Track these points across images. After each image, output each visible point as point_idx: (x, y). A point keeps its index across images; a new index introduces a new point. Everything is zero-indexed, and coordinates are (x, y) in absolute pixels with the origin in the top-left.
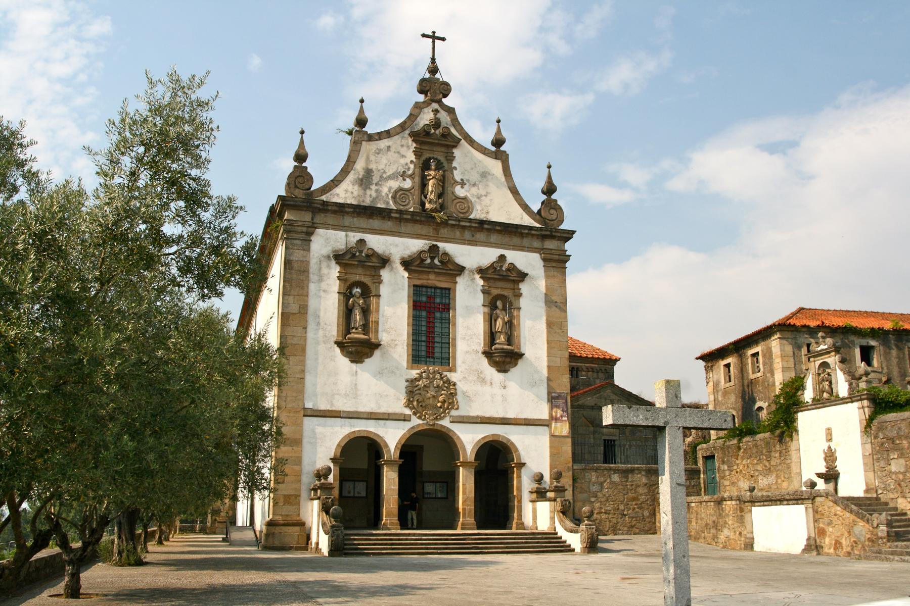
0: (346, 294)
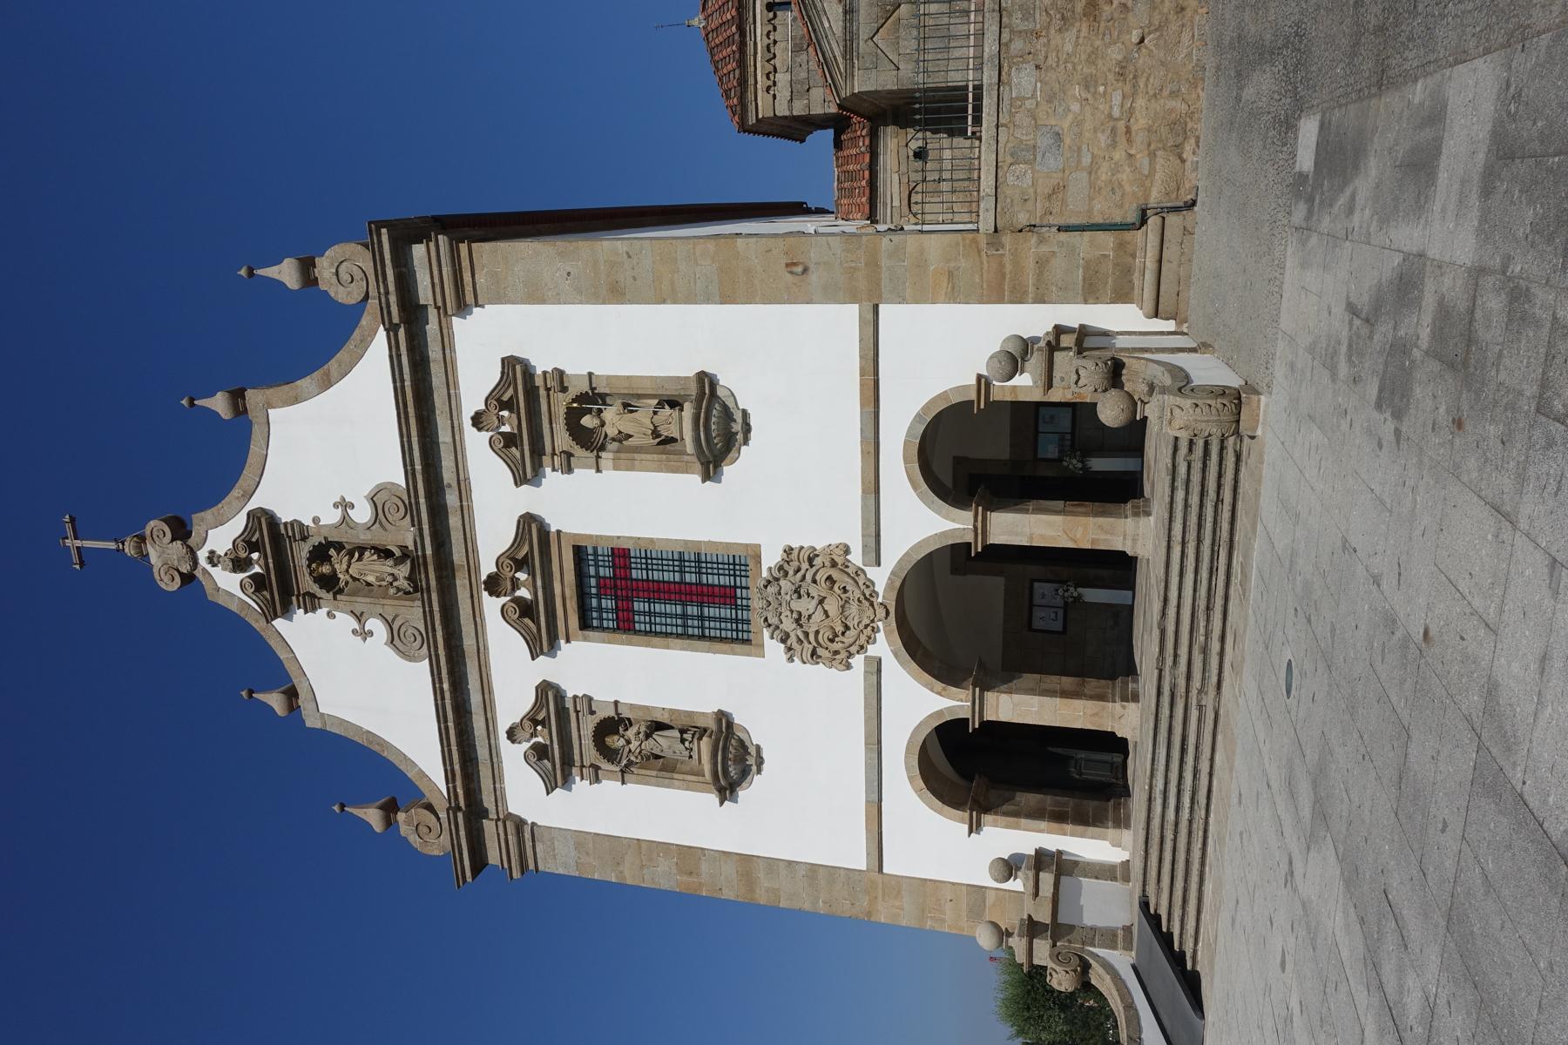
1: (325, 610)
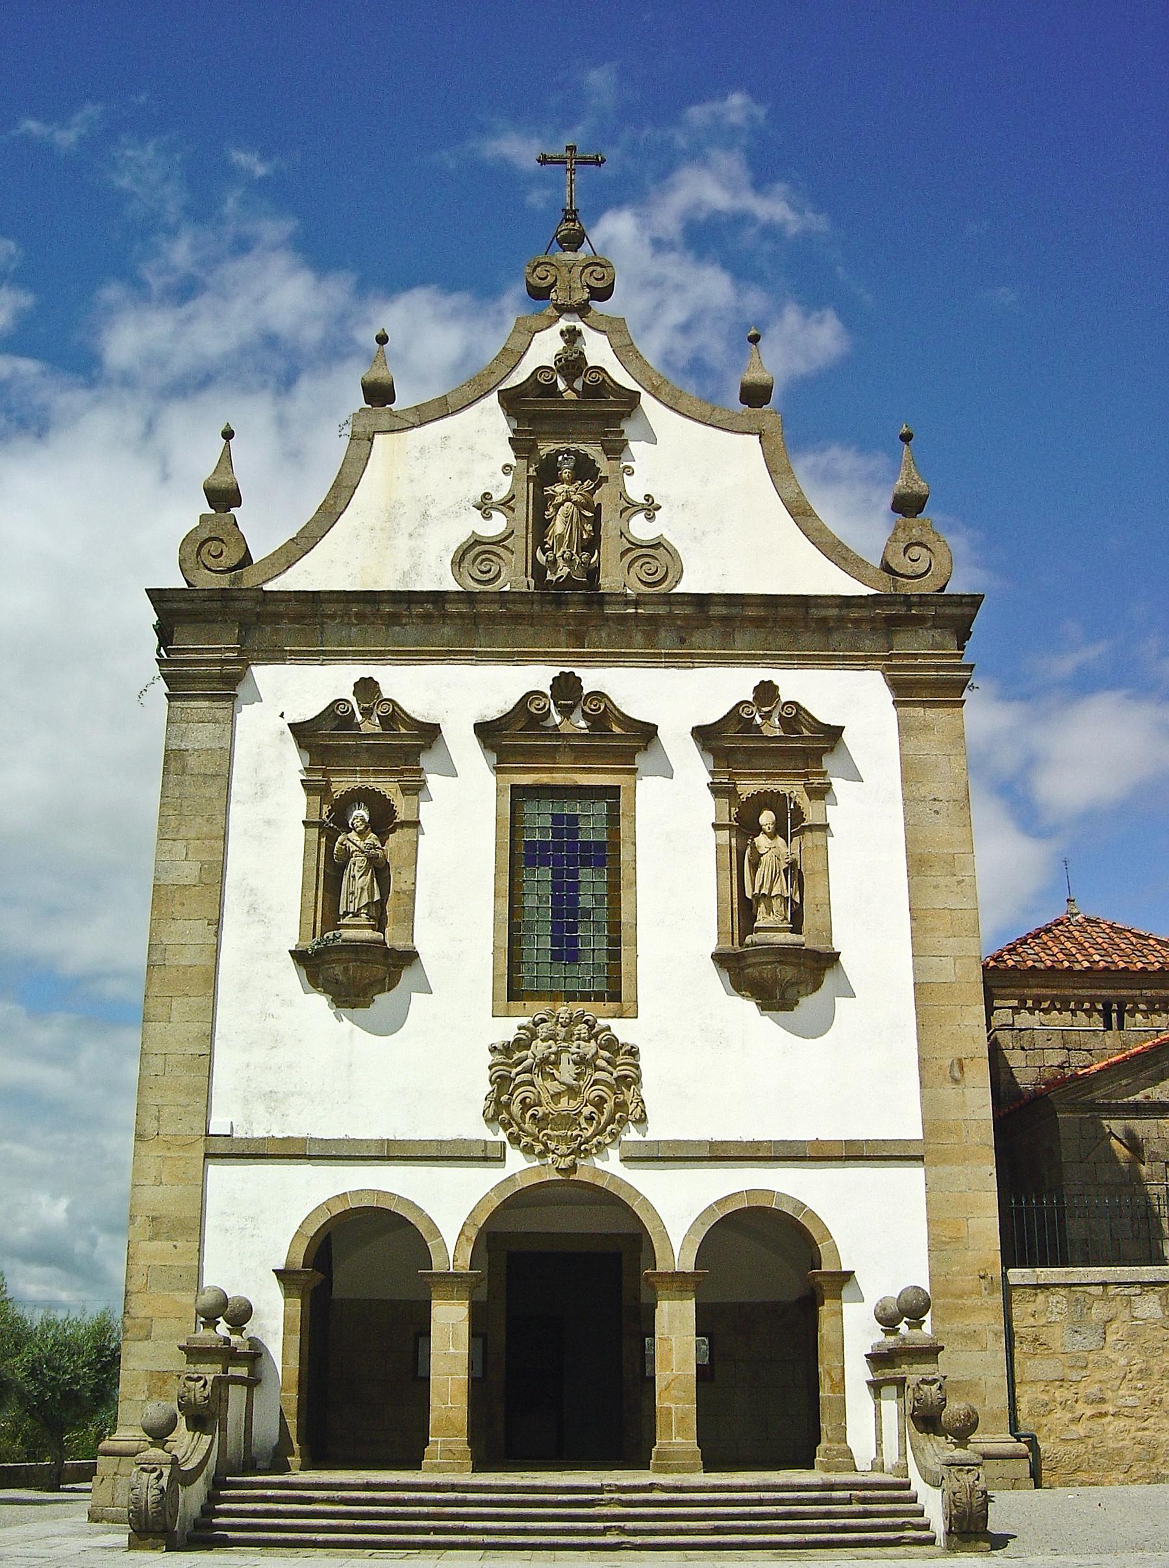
0: (328, 825)
1: (514, 462)
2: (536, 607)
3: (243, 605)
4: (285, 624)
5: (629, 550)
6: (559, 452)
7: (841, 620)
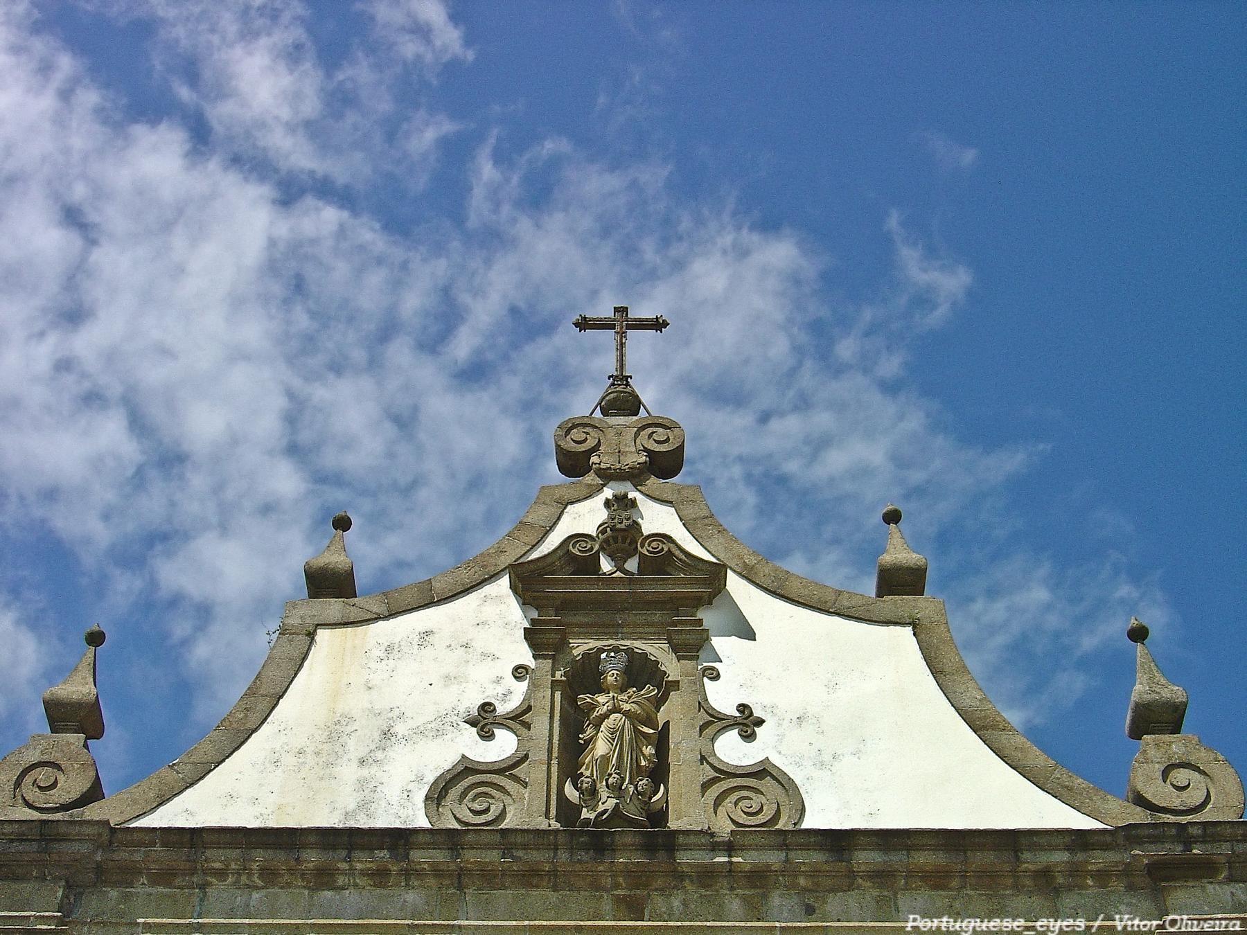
2: (563, 856)
3: (76, 846)
4: (142, 888)
5: (714, 781)
6: (601, 650)
7: (1076, 871)
